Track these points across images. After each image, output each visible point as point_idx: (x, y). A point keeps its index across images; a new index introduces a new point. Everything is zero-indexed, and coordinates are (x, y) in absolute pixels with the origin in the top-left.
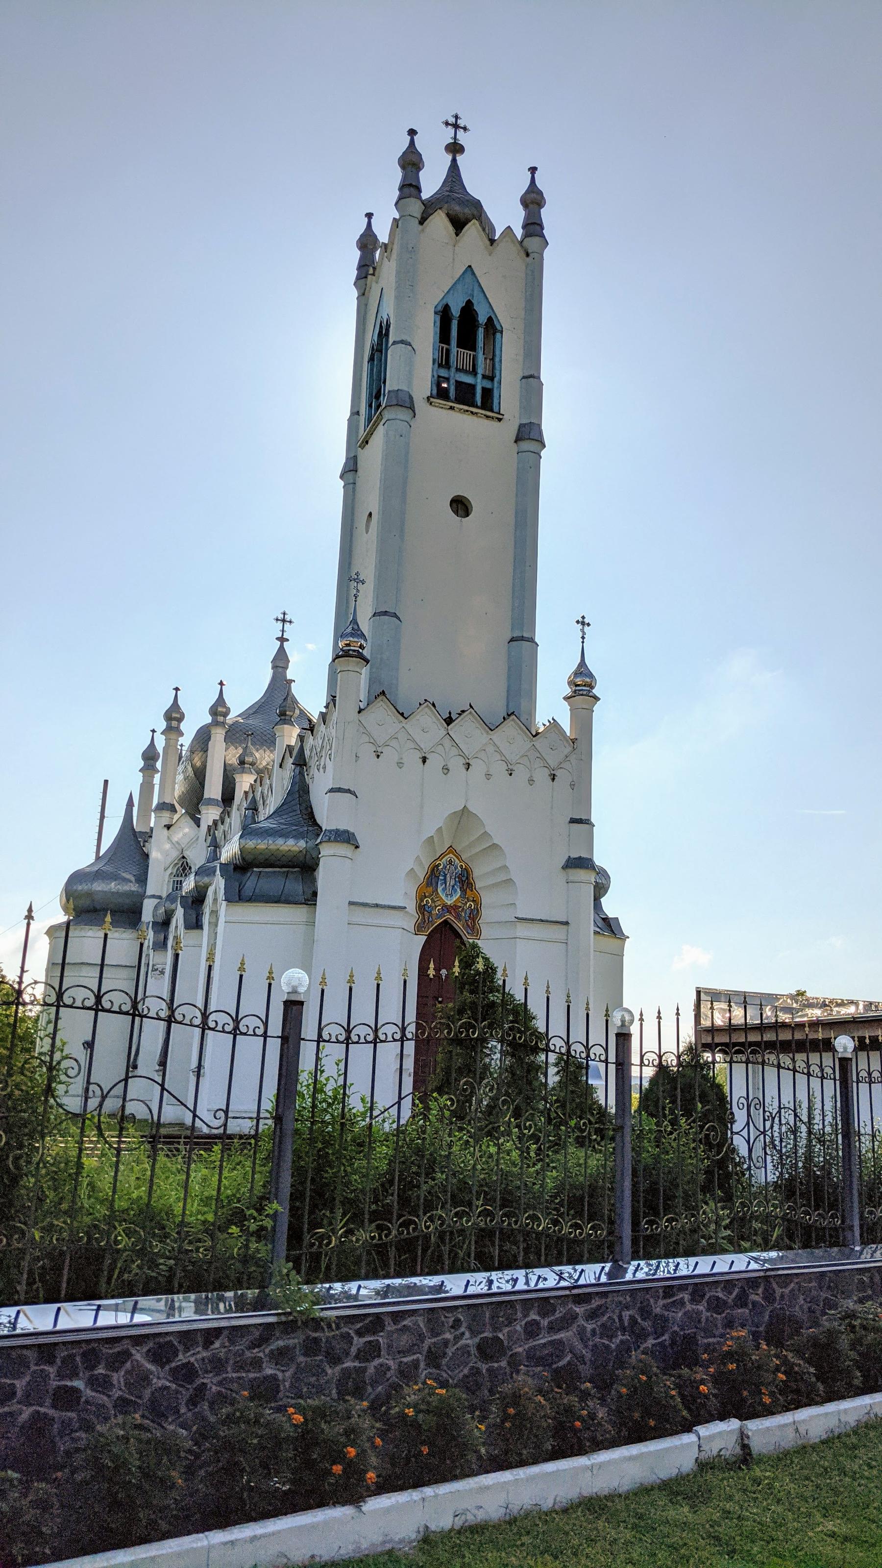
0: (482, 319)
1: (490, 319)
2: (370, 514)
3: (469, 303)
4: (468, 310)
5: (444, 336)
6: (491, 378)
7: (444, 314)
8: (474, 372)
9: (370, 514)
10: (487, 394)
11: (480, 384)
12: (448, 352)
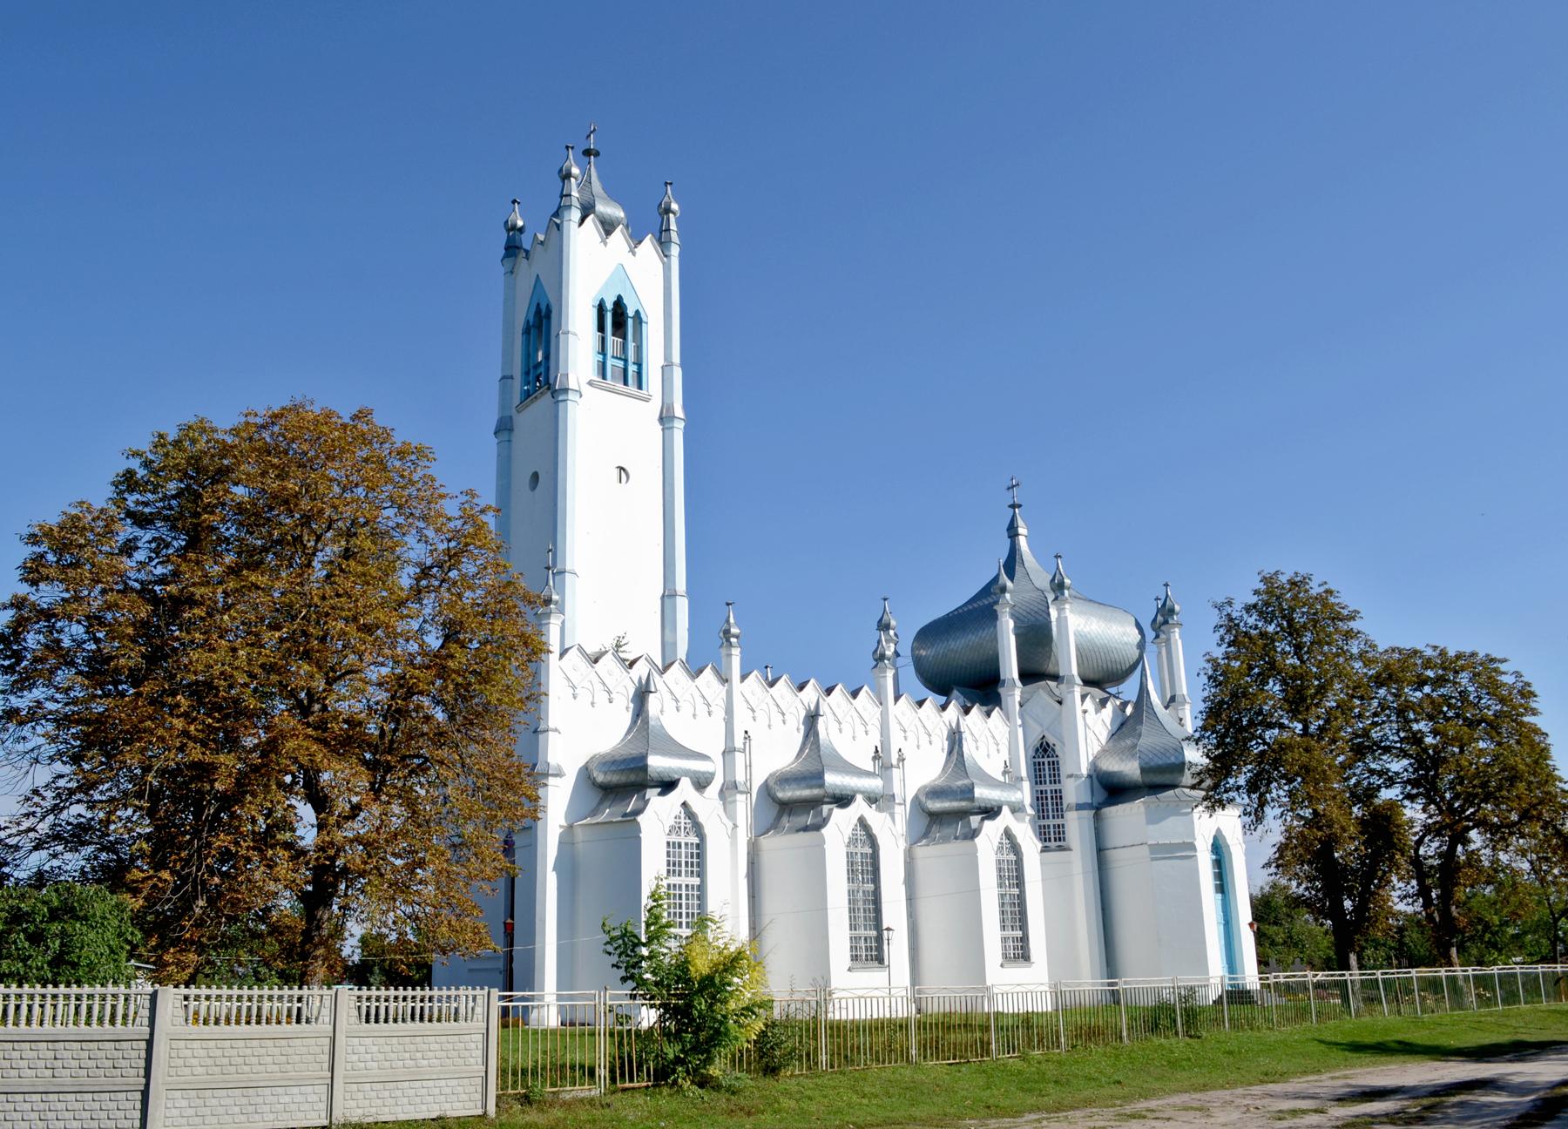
0: (631, 313)
1: (637, 312)
2: (535, 477)
3: (620, 299)
4: (619, 304)
5: (601, 328)
6: (640, 365)
7: (601, 309)
8: (626, 361)
9: (535, 477)
10: (639, 374)
11: (632, 368)
12: (603, 340)
